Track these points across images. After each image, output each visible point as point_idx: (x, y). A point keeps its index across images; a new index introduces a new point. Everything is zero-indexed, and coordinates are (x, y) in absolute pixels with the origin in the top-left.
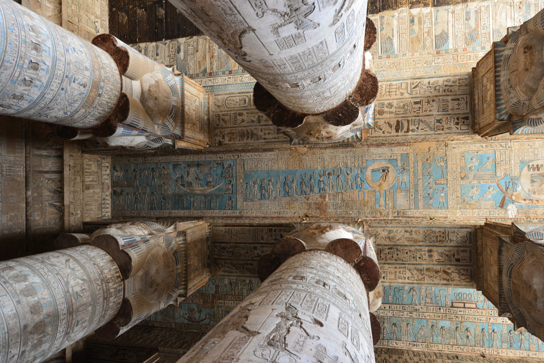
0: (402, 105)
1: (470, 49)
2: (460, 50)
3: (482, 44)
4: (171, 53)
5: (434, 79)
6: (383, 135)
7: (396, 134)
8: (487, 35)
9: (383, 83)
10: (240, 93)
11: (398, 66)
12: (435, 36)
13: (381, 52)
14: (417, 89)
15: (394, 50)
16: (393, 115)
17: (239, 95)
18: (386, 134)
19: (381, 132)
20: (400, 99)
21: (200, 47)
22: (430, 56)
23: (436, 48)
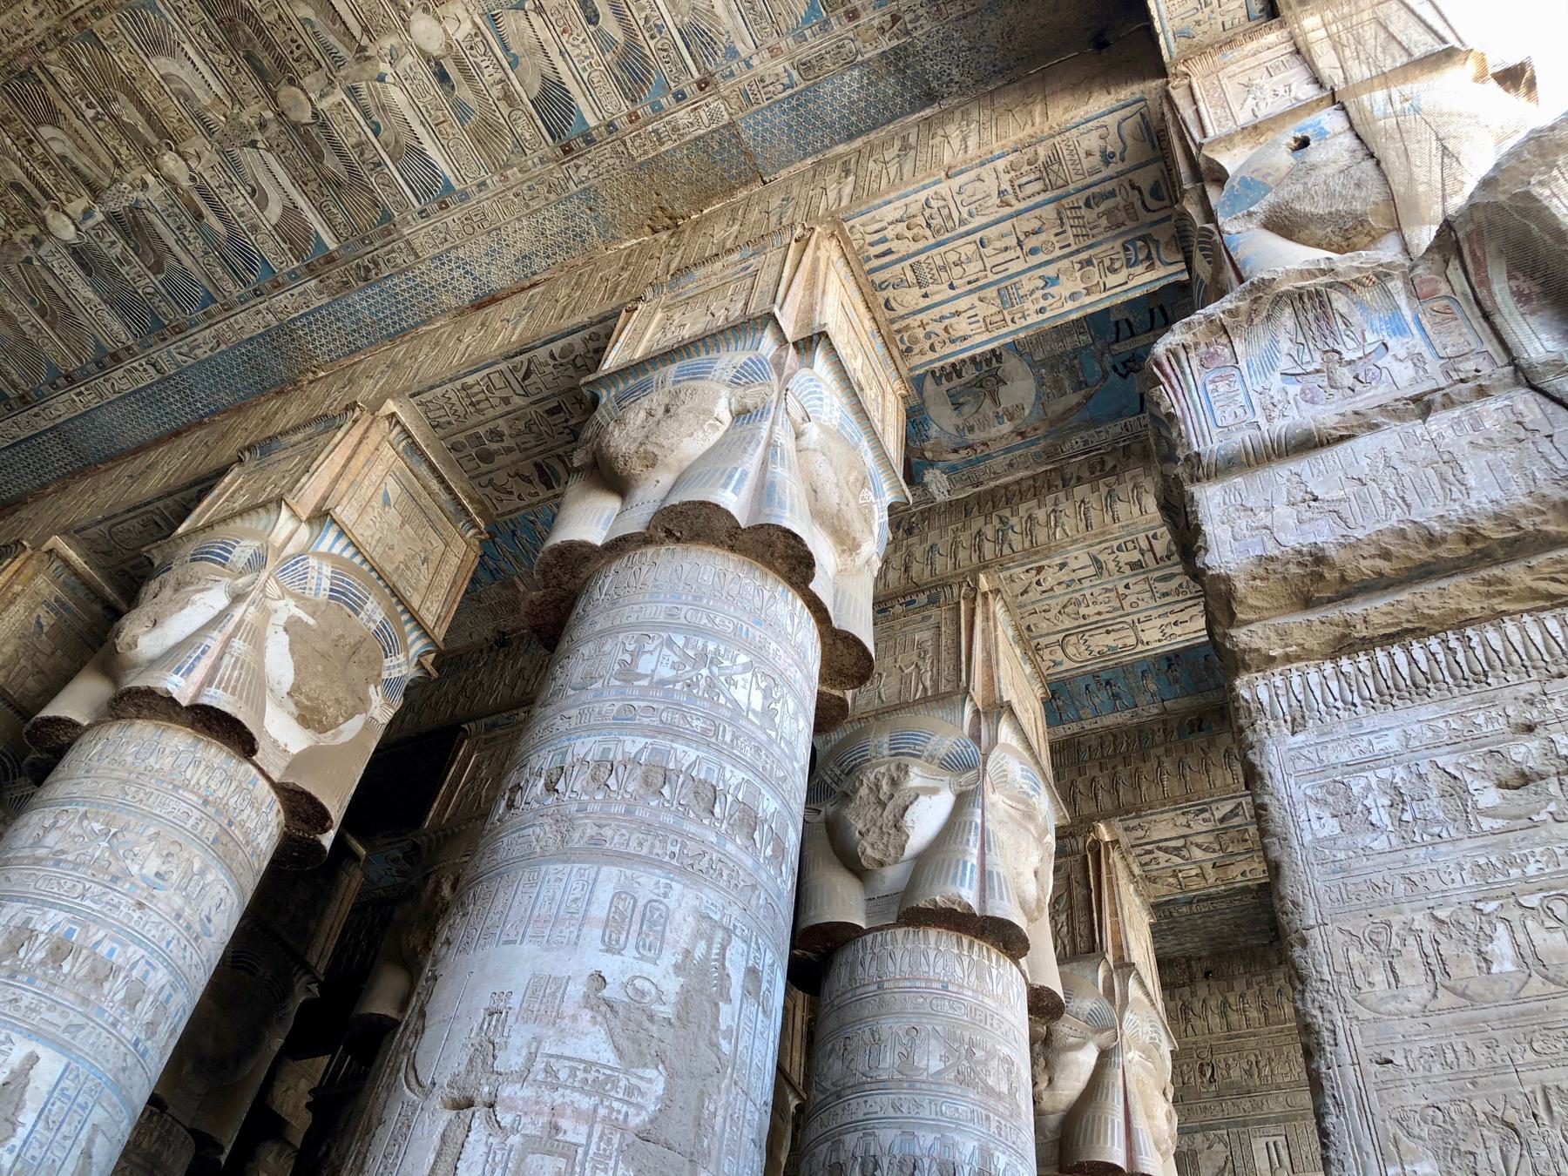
0: (521, 425)
1: (644, 110)
2: (622, 122)
5: (561, 343)
6: (523, 504)
7: (550, 493)
9: (445, 387)
10: (129, 511)
11: (486, 224)
12: (532, 102)
13: (416, 196)
14: (533, 378)
15: (447, 181)
16: (516, 455)
17: (131, 514)
18: (528, 500)
19: (515, 497)
20: (509, 413)
23: (554, 140)
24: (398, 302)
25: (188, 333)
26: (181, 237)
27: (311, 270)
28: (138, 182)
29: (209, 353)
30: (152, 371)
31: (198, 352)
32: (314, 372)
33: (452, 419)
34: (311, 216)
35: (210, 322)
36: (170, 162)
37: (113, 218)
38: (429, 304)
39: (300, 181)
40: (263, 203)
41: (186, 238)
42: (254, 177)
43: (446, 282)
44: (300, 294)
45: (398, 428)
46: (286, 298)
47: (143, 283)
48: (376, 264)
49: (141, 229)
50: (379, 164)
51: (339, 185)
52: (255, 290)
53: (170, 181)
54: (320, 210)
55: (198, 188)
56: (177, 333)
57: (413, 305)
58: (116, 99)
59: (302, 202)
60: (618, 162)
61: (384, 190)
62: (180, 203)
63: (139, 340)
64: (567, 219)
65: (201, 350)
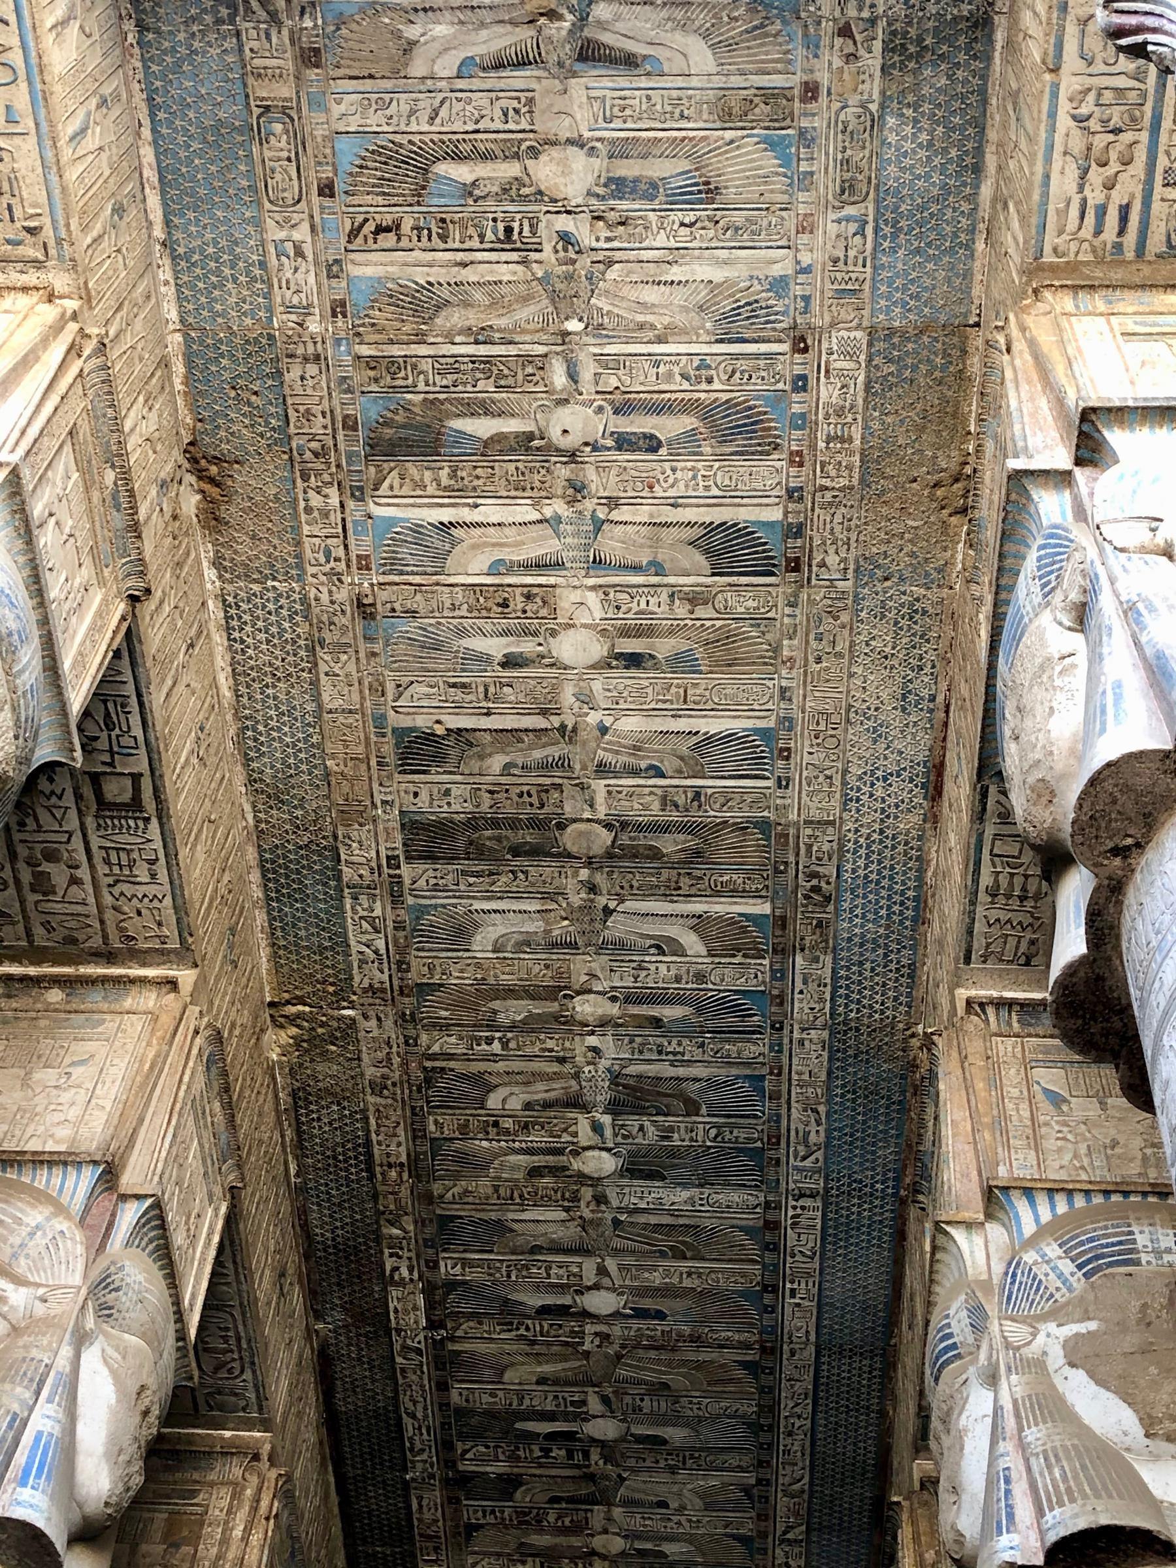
3: (780, 386)
4: (662, 1464)
8: (742, 364)
12: (713, 574)
15: (756, 731)
21: (649, 1376)
22: (804, 596)
24: (878, 883)
25: (784, 1131)
26: (671, 1057)
27: (782, 951)
28: (590, 1054)
29: (821, 1129)
30: (807, 1202)
31: (813, 1138)
32: (913, 1035)
33: (1029, 935)
34: (718, 908)
35: (783, 1100)
36: (586, 1008)
37: (615, 1108)
38: (901, 848)
39: (671, 892)
40: (678, 949)
41: (674, 1054)
42: (642, 936)
43: (883, 811)
44: (805, 982)
45: (990, 1011)
46: (801, 1001)
47: (701, 1133)
48: (815, 875)
49: (641, 1090)
50: (697, 795)
51: (698, 853)
52: (772, 1027)
53: (605, 1023)
54: (718, 894)
55: (628, 1000)
56: (778, 1143)
57: (892, 868)
58: (495, 1012)
59: (697, 907)
60: (843, 510)
61: (731, 809)
62: (631, 1031)
63: (764, 1187)
64: (883, 616)
65: (813, 1134)
